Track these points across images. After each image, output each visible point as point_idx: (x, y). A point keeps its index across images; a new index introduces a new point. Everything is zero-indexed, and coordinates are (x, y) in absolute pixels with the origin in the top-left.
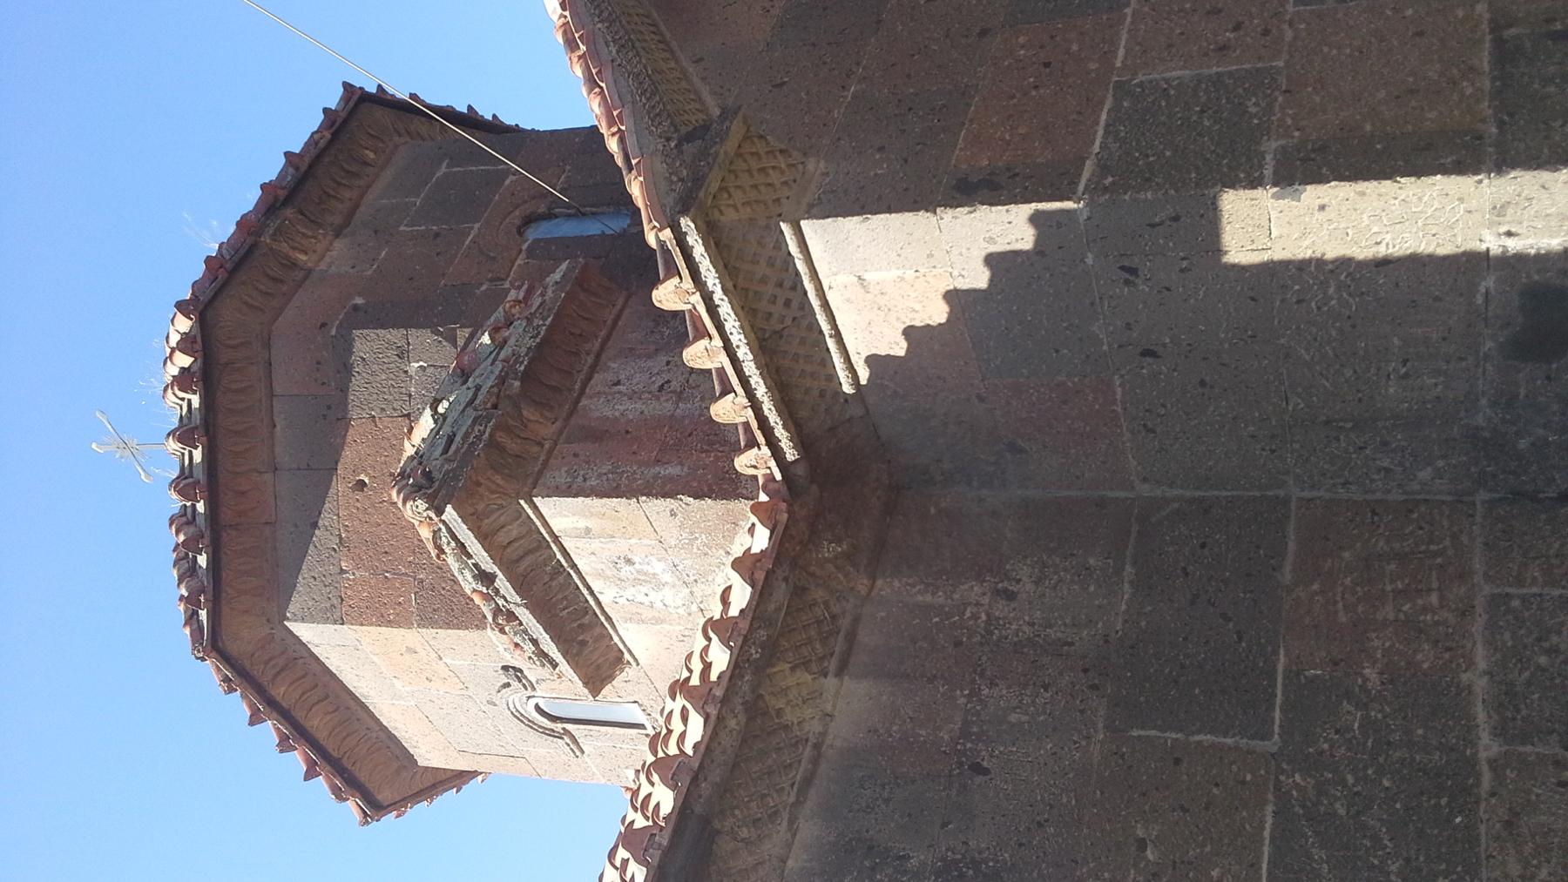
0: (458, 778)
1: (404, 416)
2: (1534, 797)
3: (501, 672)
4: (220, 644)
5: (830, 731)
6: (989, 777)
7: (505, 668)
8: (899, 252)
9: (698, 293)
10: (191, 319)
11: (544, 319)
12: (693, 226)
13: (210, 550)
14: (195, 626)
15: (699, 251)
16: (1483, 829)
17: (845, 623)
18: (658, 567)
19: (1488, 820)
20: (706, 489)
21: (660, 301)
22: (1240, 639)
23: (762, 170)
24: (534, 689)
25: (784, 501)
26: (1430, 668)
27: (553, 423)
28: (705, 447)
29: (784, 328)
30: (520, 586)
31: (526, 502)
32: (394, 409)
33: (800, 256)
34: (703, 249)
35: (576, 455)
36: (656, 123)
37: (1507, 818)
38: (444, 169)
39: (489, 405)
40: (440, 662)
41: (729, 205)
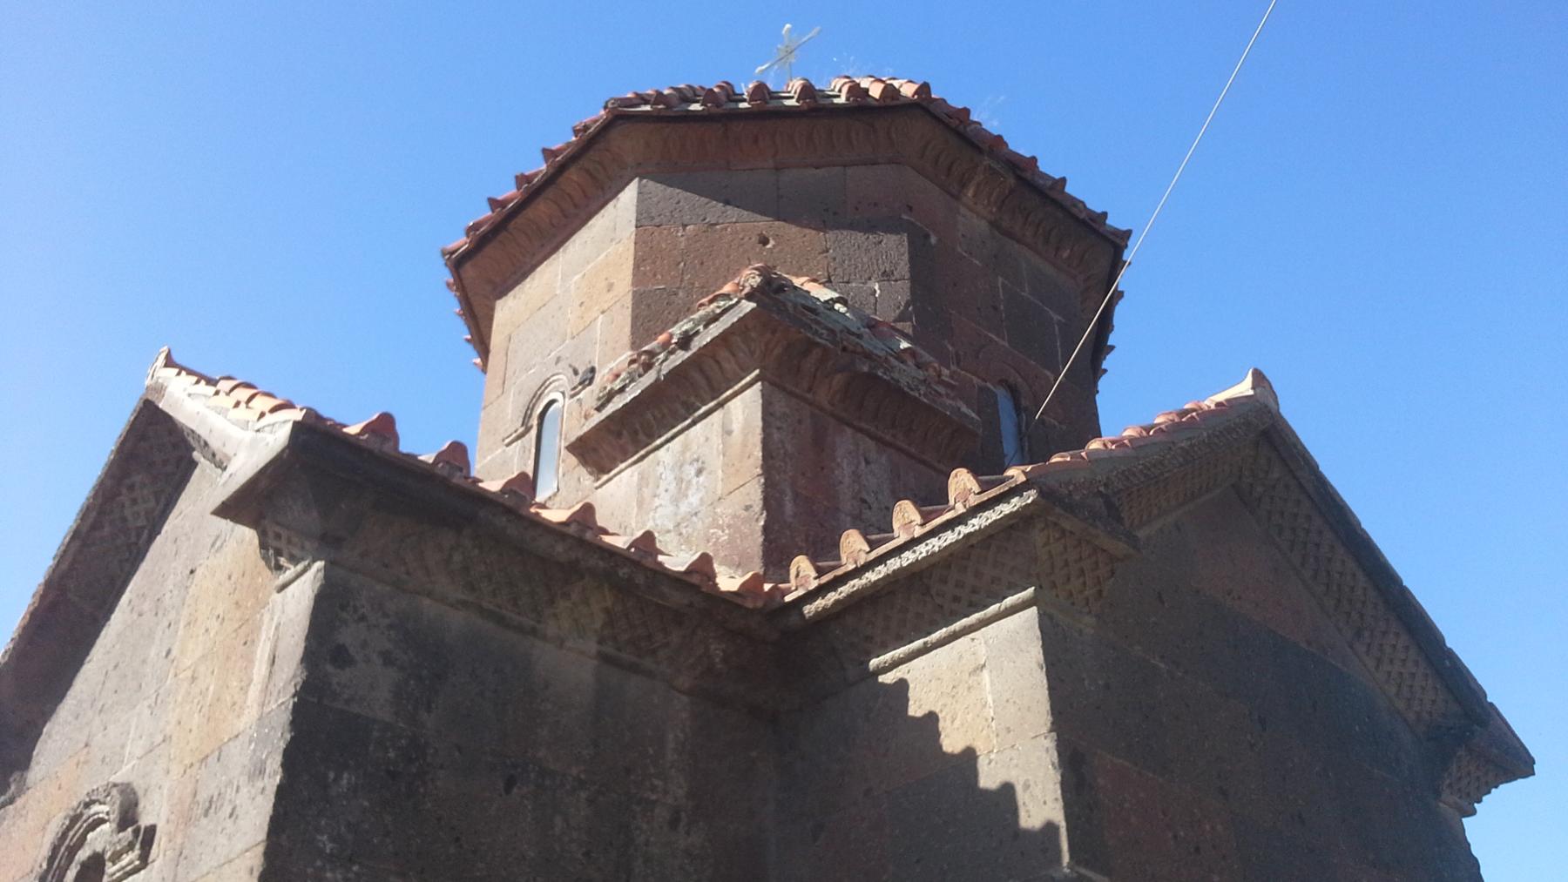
0: (481, 342)
1: (829, 277)
3: (589, 366)
4: (620, 122)
7: (593, 370)
8: (1011, 701)
9: (965, 510)
10: (913, 96)
11: (925, 395)
12: (1029, 501)
13: (706, 113)
14: (635, 102)
15: (1005, 509)
17: (648, 663)
18: (694, 499)
21: (956, 475)
23: (1082, 572)
25: (765, 605)
27: (829, 402)
28: (810, 539)
29: (932, 596)
30: (677, 374)
31: (757, 376)
32: (835, 269)
33: (1003, 608)
34: (1007, 512)
35: (800, 422)
36: (1119, 476)
38: (1056, 317)
39: (845, 343)
40: (599, 312)
41: (1048, 538)
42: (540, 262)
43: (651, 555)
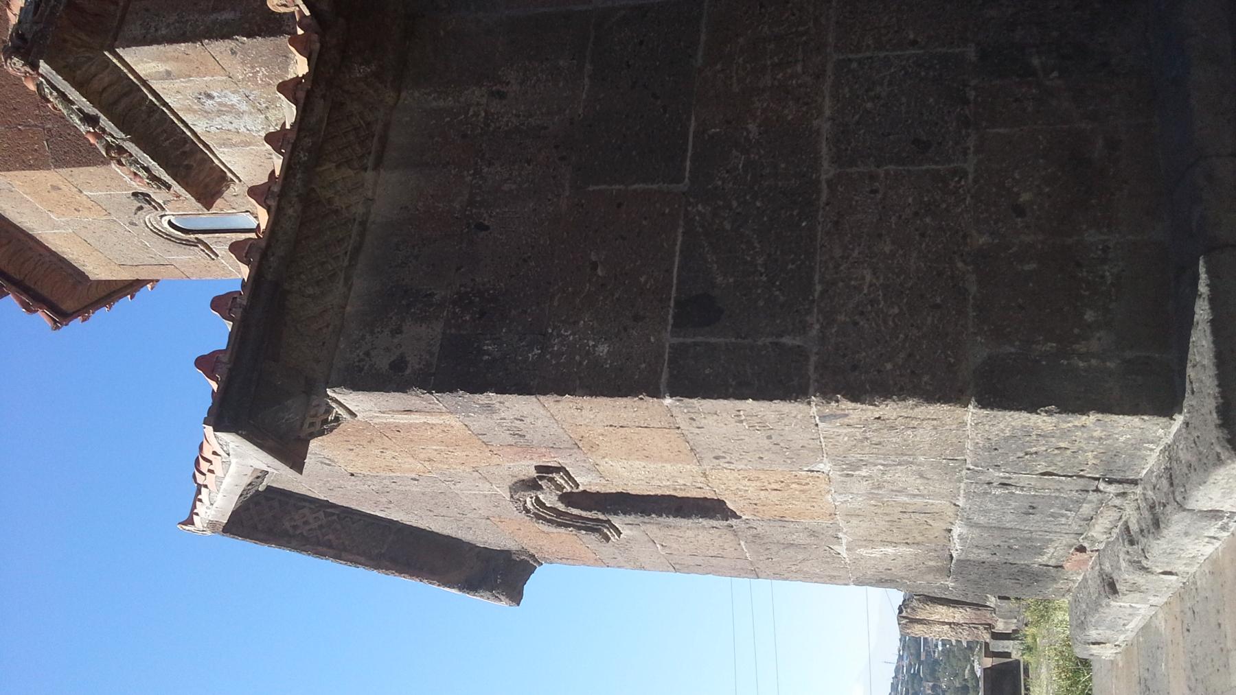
0: (132, 287)
2: (854, 203)
3: (132, 198)
5: (372, 211)
6: (489, 231)
7: (135, 194)
16: (819, 228)
18: (234, 99)
19: (823, 222)
20: (256, 29)
22: (665, 112)
24: (163, 209)
25: (316, 33)
26: (792, 119)
31: (110, 53)
35: (147, 10)
37: (835, 219)
40: (81, 195)
42: (47, 248)
43: (285, 134)
